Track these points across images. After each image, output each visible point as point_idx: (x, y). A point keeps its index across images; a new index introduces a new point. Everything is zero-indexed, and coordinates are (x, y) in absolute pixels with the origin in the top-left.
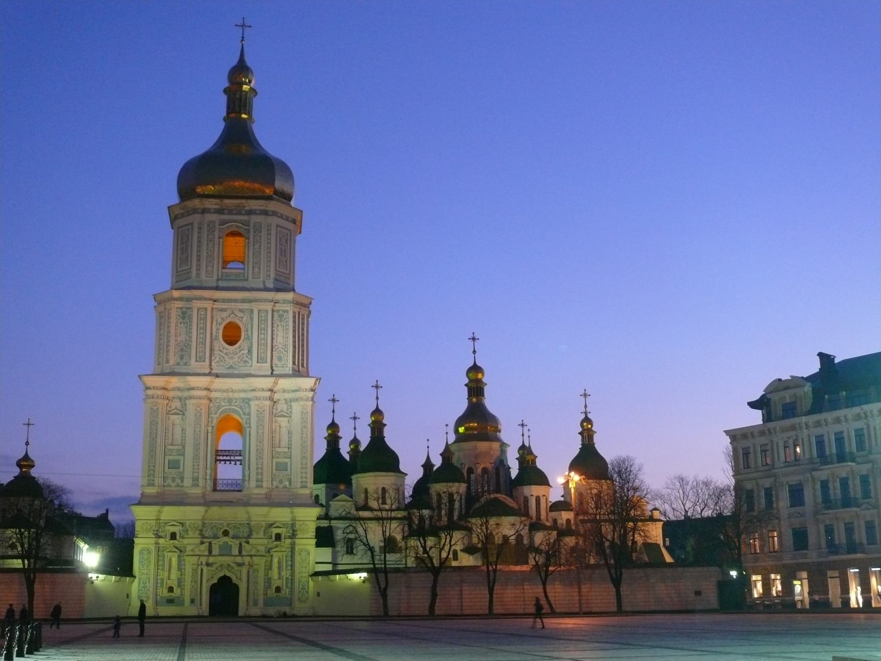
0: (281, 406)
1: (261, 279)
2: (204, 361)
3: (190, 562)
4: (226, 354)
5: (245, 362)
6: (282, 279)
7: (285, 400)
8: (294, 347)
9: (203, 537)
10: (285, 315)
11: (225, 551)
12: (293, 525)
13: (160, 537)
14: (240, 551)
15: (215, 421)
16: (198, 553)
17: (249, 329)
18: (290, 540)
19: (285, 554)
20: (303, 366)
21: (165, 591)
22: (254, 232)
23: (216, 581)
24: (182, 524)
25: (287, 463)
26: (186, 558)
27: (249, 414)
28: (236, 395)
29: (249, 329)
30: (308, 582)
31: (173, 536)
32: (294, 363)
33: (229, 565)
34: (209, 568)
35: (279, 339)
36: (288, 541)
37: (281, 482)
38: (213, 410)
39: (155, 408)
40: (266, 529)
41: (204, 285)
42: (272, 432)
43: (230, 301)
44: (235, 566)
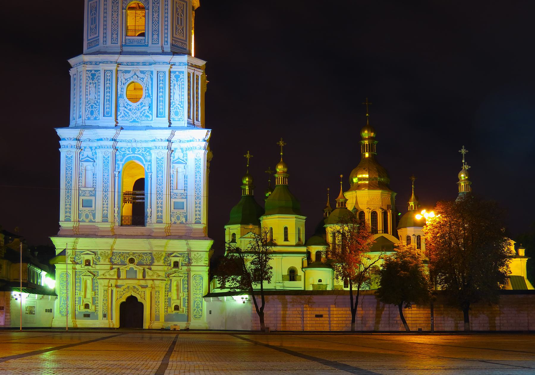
0: (178, 154)
1: (160, 45)
2: (111, 116)
3: (102, 284)
4: (130, 110)
5: (147, 116)
6: (180, 45)
7: (182, 149)
8: (189, 103)
9: (112, 263)
10: (181, 76)
11: (132, 275)
12: (189, 255)
13: (77, 263)
14: (144, 276)
15: (121, 167)
16: (108, 277)
17: (150, 88)
18: (186, 268)
19: (182, 278)
20: (197, 120)
21: (82, 307)
23: (124, 300)
24: (95, 253)
25: (183, 203)
26: (98, 280)
27: (150, 161)
28: (139, 145)
29: (150, 88)
30: (202, 302)
31: (88, 263)
32: (189, 117)
33: (134, 287)
34: (118, 289)
35: (176, 97)
36: (185, 268)
37: (178, 218)
38: (119, 157)
39: (69, 156)
40: (165, 258)
41: (108, 51)
42: (170, 176)
43: (132, 64)
44: (140, 288)
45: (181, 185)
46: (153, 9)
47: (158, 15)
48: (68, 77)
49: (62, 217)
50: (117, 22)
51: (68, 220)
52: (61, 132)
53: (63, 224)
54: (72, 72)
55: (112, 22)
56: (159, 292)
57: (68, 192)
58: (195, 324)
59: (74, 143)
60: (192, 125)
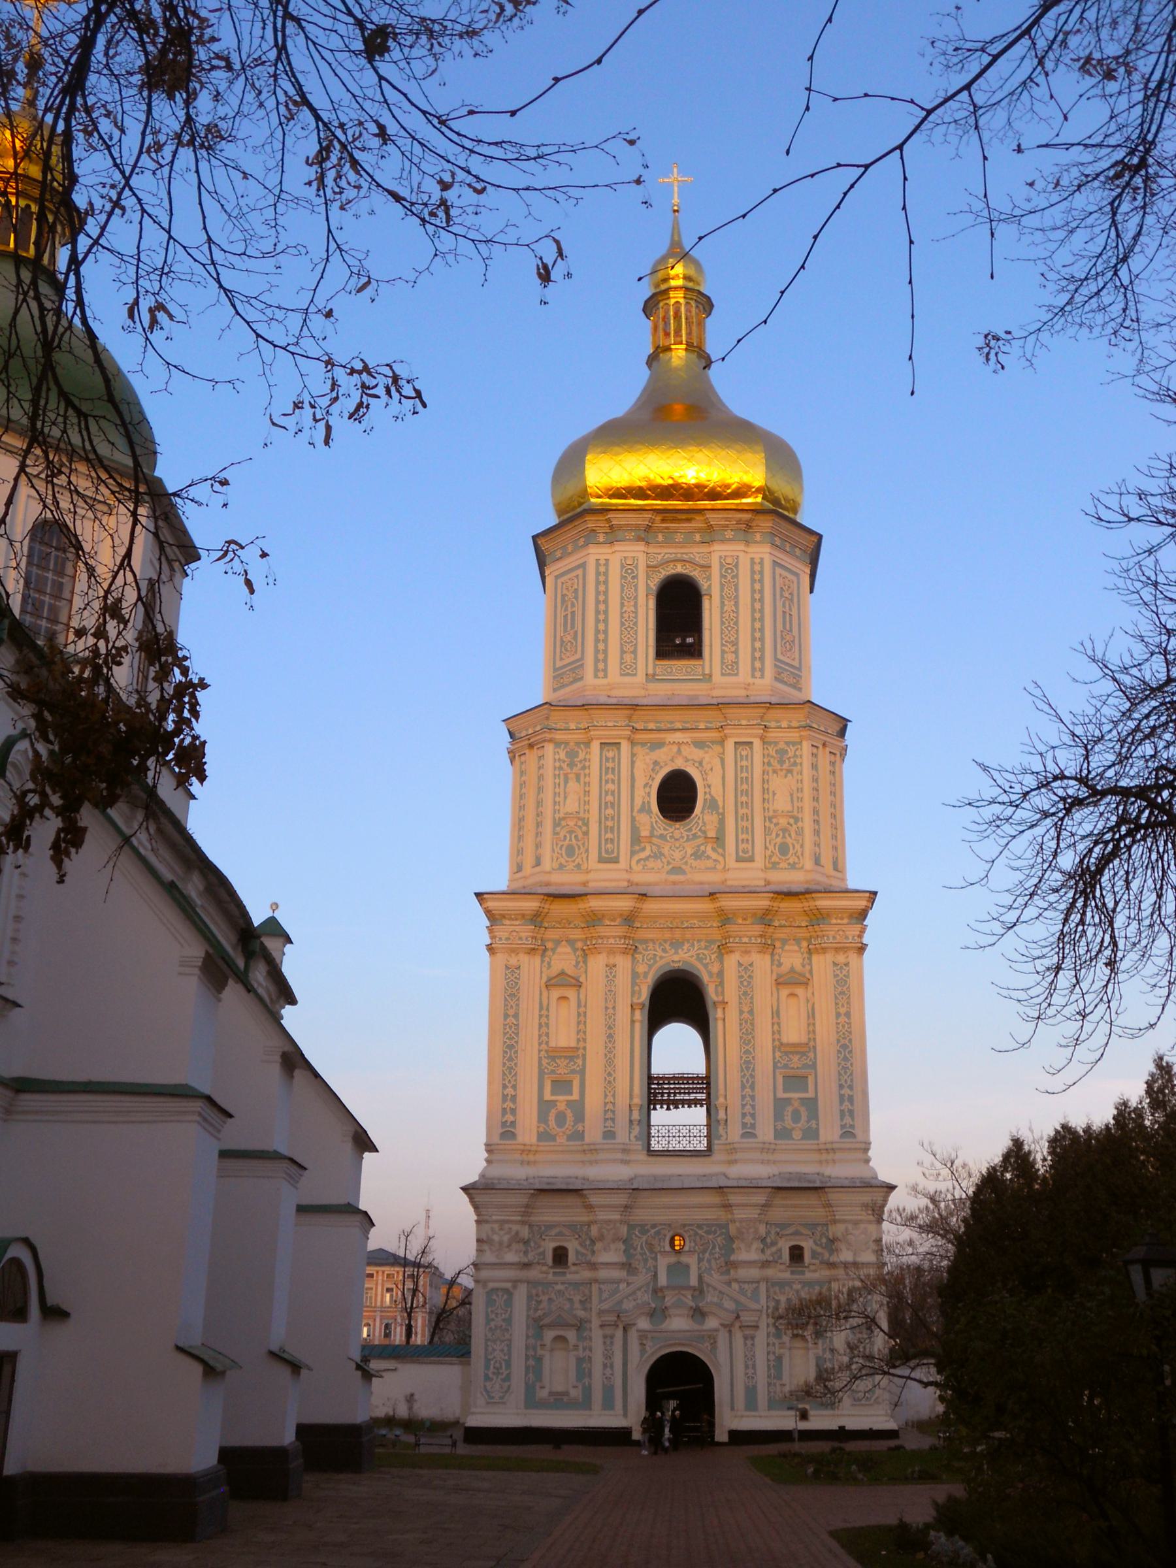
22: (722, 576)
46: (722, 590)
47: (736, 604)
50: (635, 624)
55: (622, 624)
56: (753, 1338)
57: (510, 1059)
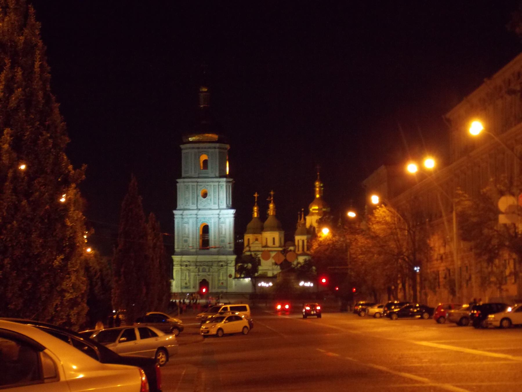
0: (222, 220)
3: (192, 274)
9: (196, 266)
11: (204, 271)
31: (186, 266)
45: (224, 233)
48: (176, 186)
49: (176, 247)
51: (178, 248)
52: (175, 212)
53: (177, 249)
54: (178, 185)
58: (229, 290)
59: (181, 216)
60: (228, 208)
